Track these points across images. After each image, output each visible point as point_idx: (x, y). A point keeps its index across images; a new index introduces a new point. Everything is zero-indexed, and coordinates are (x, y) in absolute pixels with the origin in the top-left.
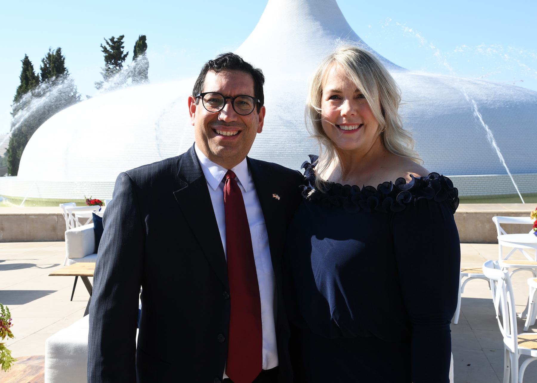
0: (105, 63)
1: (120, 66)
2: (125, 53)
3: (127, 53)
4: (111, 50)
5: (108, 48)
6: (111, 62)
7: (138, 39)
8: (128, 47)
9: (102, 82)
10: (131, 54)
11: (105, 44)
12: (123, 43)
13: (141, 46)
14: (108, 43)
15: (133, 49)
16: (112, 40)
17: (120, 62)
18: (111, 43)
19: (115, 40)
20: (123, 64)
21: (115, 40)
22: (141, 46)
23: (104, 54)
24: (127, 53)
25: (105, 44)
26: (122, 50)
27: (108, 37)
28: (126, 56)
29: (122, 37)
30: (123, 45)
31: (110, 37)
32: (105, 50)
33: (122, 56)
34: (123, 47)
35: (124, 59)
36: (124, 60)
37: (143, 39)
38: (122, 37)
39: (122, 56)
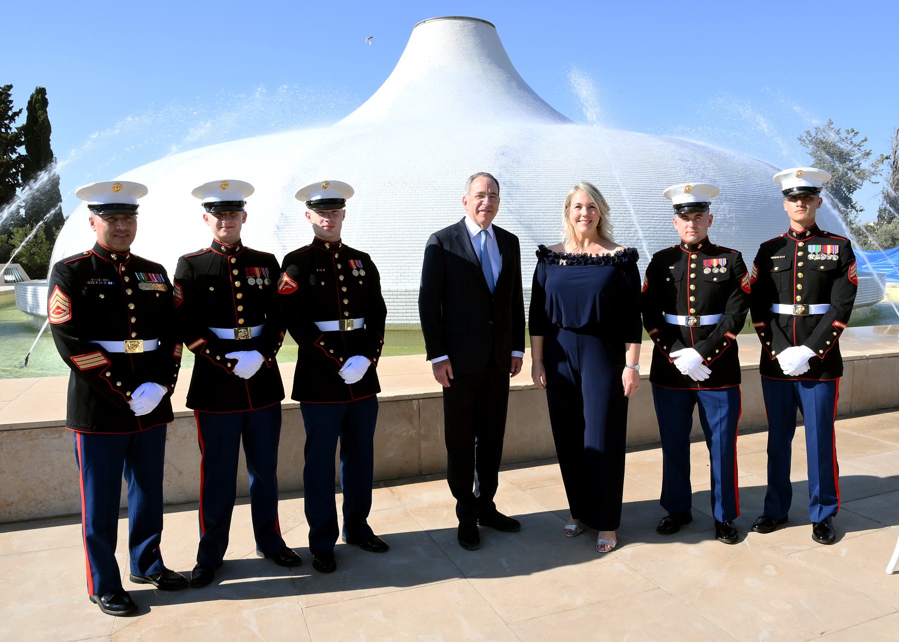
1: (8, 127)
2: (14, 110)
3: (21, 111)
7: (33, 91)
8: (20, 101)
10: (25, 114)
12: (10, 95)
13: (39, 102)
15: (25, 105)
17: (7, 122)
20: (12, 125)
22: (39, 102)
24: (21, 111)
28: (17, 114)
29: (10, 87)
30: (10, 99)
33: (10, 113)
34: (11, 102)
35: (12, 119)
37: (41, 92)
38: (10, 87)
39: (10, 113)
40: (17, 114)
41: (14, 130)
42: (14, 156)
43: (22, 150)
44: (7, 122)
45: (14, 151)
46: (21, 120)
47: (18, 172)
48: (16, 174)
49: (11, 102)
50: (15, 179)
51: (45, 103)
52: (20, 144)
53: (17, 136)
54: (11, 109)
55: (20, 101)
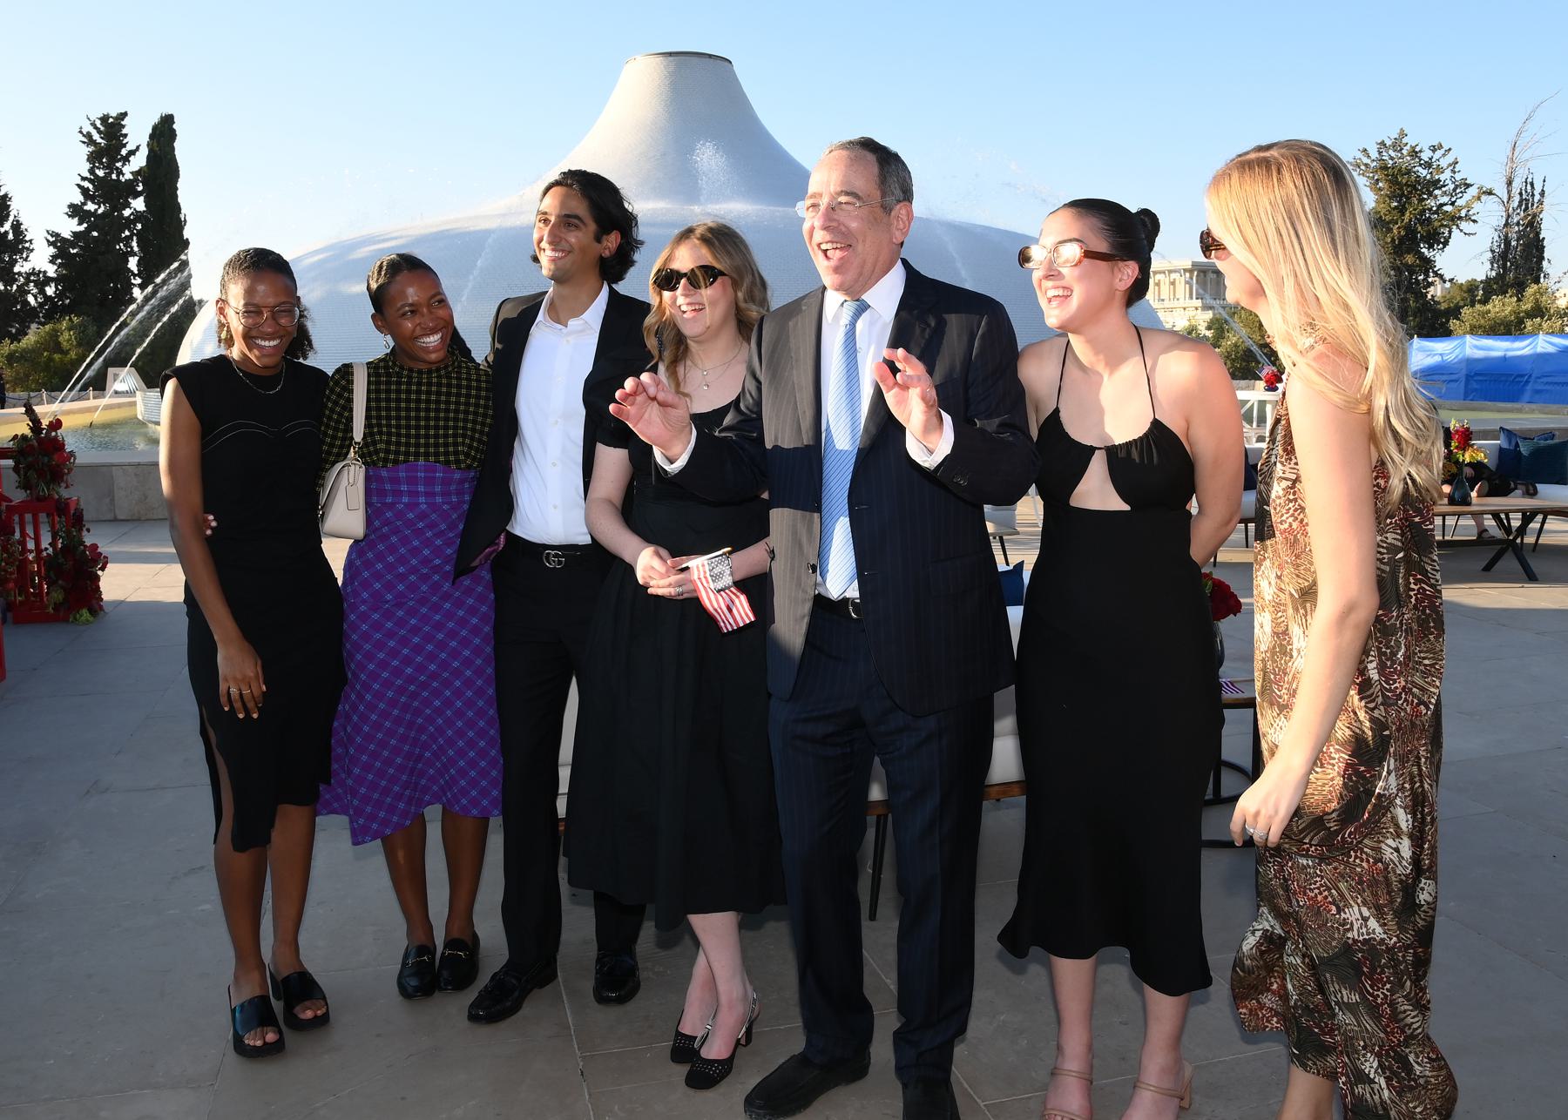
0: (88, 166)
1: (120, 173)
2: (130, 147)
5: (96, 137)
7: (156, 119)
8: (137, 135)
11: (88, 128)
16: (104, 119)
17: (119, 165)
22: (164, 132)
23: (86, 150)
25: (88, 128)
27: (96, 115)
28: (132, 153)
29: (125, 115)
30: (124, 131)
32: (89, 140)
33: (124, 152)
35: (126, 159)
38: (125, 115)
39: (124, 152)
40: (132, 153)
41: (128, 176)
42: (127, 212)
43: (139, 204)
44: (119, 165)
45: (128, 205)
46: (139, 161)
47: (132, 234)
48: (129, 238)
50: (128, 245)
52: (136, 195)
53: (130, 184)
55: (137, 135)
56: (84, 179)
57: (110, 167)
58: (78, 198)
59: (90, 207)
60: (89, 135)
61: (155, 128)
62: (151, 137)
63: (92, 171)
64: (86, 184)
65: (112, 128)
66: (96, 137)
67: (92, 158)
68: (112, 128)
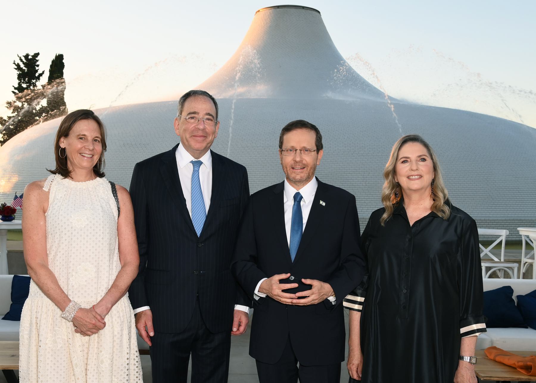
0: (18, 81)
1: (35, 85)
2: (40, 72)
3: (43, 72)
4: (24, 68)
5: (22, 66)
6: (24, 80)
8: (44, 66)
9: (15, 102)
10: (47, 75)
11: (18, 61)
12: (37, 61)
13: (58, 66)
14: (21, 60)
15: (48, 68)
16: (26, 56)
18: (25, 61)
19: (30, 57)
20: (37, 83)
21: (30, 57)
23: (17, 72)
24: (43, 72)
25: (18, 61)
26: (37, 68)
27: (22, 54)
28: (41, 75)
29: (37, 55)
30: (37, 63)
31: (25, 54)
32: (18, 68)
33: (37, 75)
34: (38, 66)
35: (38, 78)
36: (39, 79)
38: (37, 55)
39: (37, 75)
49: (38, 66)
51: (62, 66)
54: (37, 71)
55: (44, 66)
56: (15, 88)
57: (30, 83)
58: (12, 98)
59: (19, 104)
60: (18, 65)
61: (53, 62)
62: (51, 66)
63: (19, 84)
64: (16, 91)
65: (31, 62)
66: (22, 66)
67: (20, 77)
68: (31, 62)
